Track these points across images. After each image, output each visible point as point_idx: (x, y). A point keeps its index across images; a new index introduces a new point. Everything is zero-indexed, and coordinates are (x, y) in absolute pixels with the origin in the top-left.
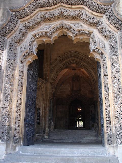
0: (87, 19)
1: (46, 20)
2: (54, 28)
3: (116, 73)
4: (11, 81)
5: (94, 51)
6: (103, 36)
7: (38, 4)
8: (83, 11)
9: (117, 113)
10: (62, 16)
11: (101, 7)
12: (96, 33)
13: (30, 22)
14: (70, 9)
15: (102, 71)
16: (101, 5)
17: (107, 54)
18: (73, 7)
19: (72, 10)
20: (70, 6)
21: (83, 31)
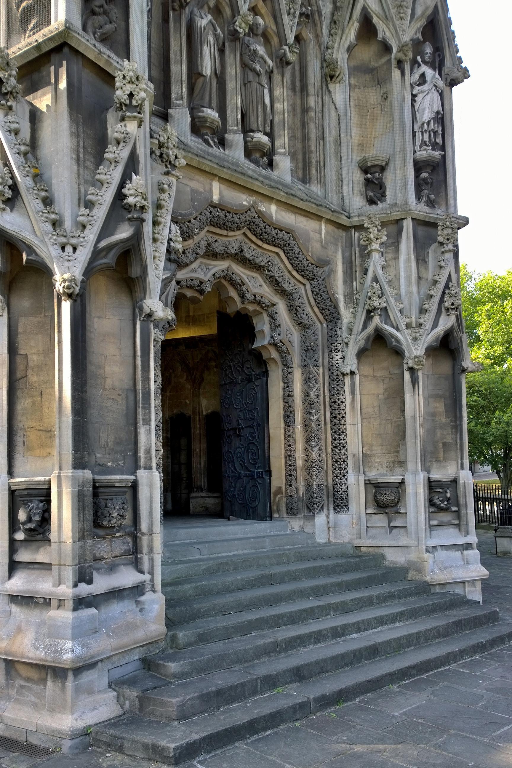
2: (214, 275)
3: (316, 397)
6: (294, 320)
7: (213, 217)
8: (276, 260)
9: (314, 465)
12: (281, 308)
13: (187, 252)
14: (255, 247)
16: (312, 264)
18: (265, 246)
19: (259, 250)
20: (260, 243)
21: (262, 297)
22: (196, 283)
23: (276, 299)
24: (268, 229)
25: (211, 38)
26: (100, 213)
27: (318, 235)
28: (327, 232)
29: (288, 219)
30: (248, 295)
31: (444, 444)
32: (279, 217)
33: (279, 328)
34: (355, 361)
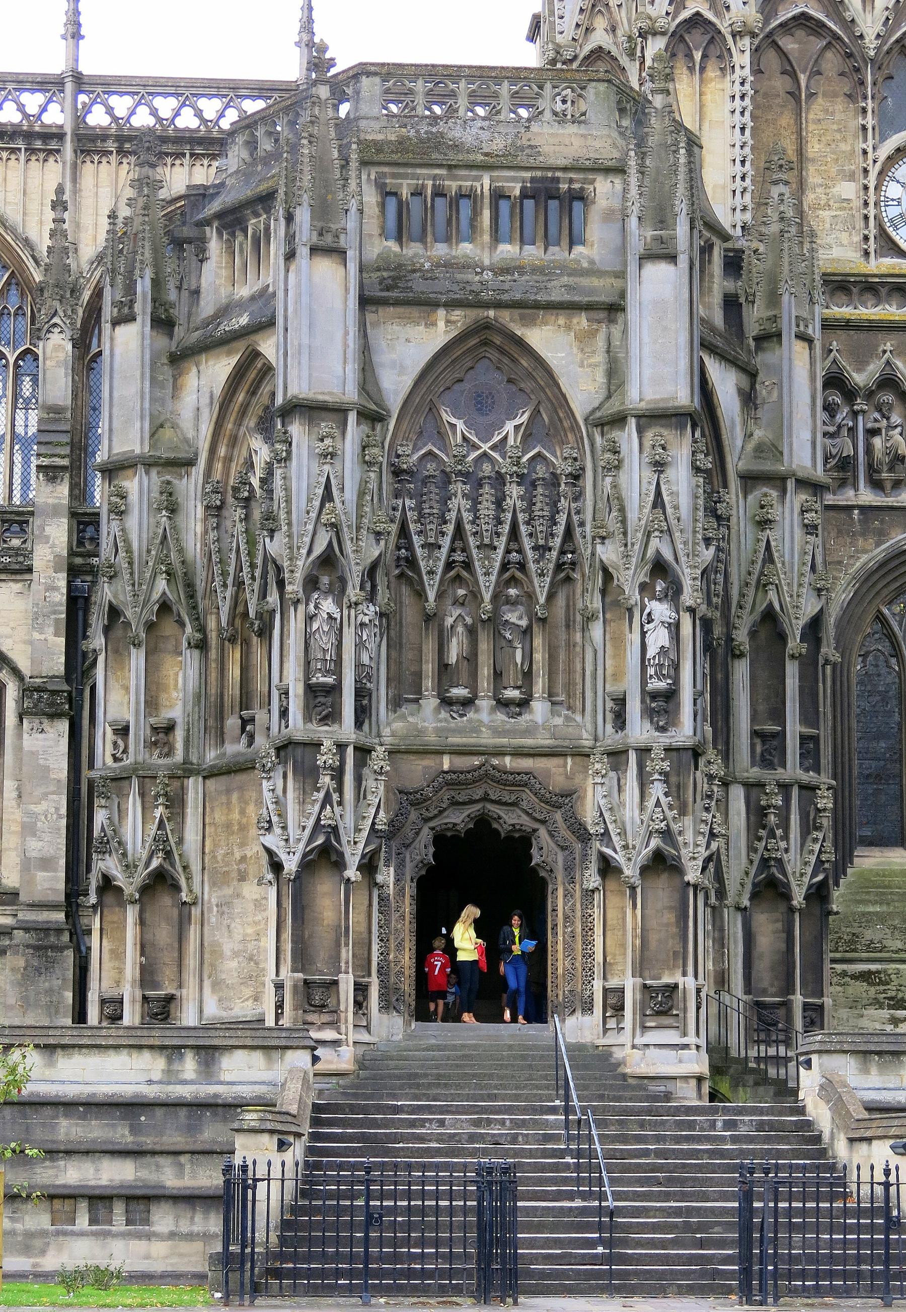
0: (530, 811)
1: (455, 803)
2: (468, 816)
4: (403, 917)
5: (538, 865)
10: (486, 798)
11: (555, 799)
15: (550, 900)
17: (560, 875)
22: (450, 826)
23: (536, 825)
24: (504, 777)
25: (460, 629)
26: (308, 832)
27: (561, 770)
28: (574, 763)
29: (526, 763)
30: (505, 826)
31: (674, 952)
32: (514, 765)
33: (545, 851)
34: (598, 878)
